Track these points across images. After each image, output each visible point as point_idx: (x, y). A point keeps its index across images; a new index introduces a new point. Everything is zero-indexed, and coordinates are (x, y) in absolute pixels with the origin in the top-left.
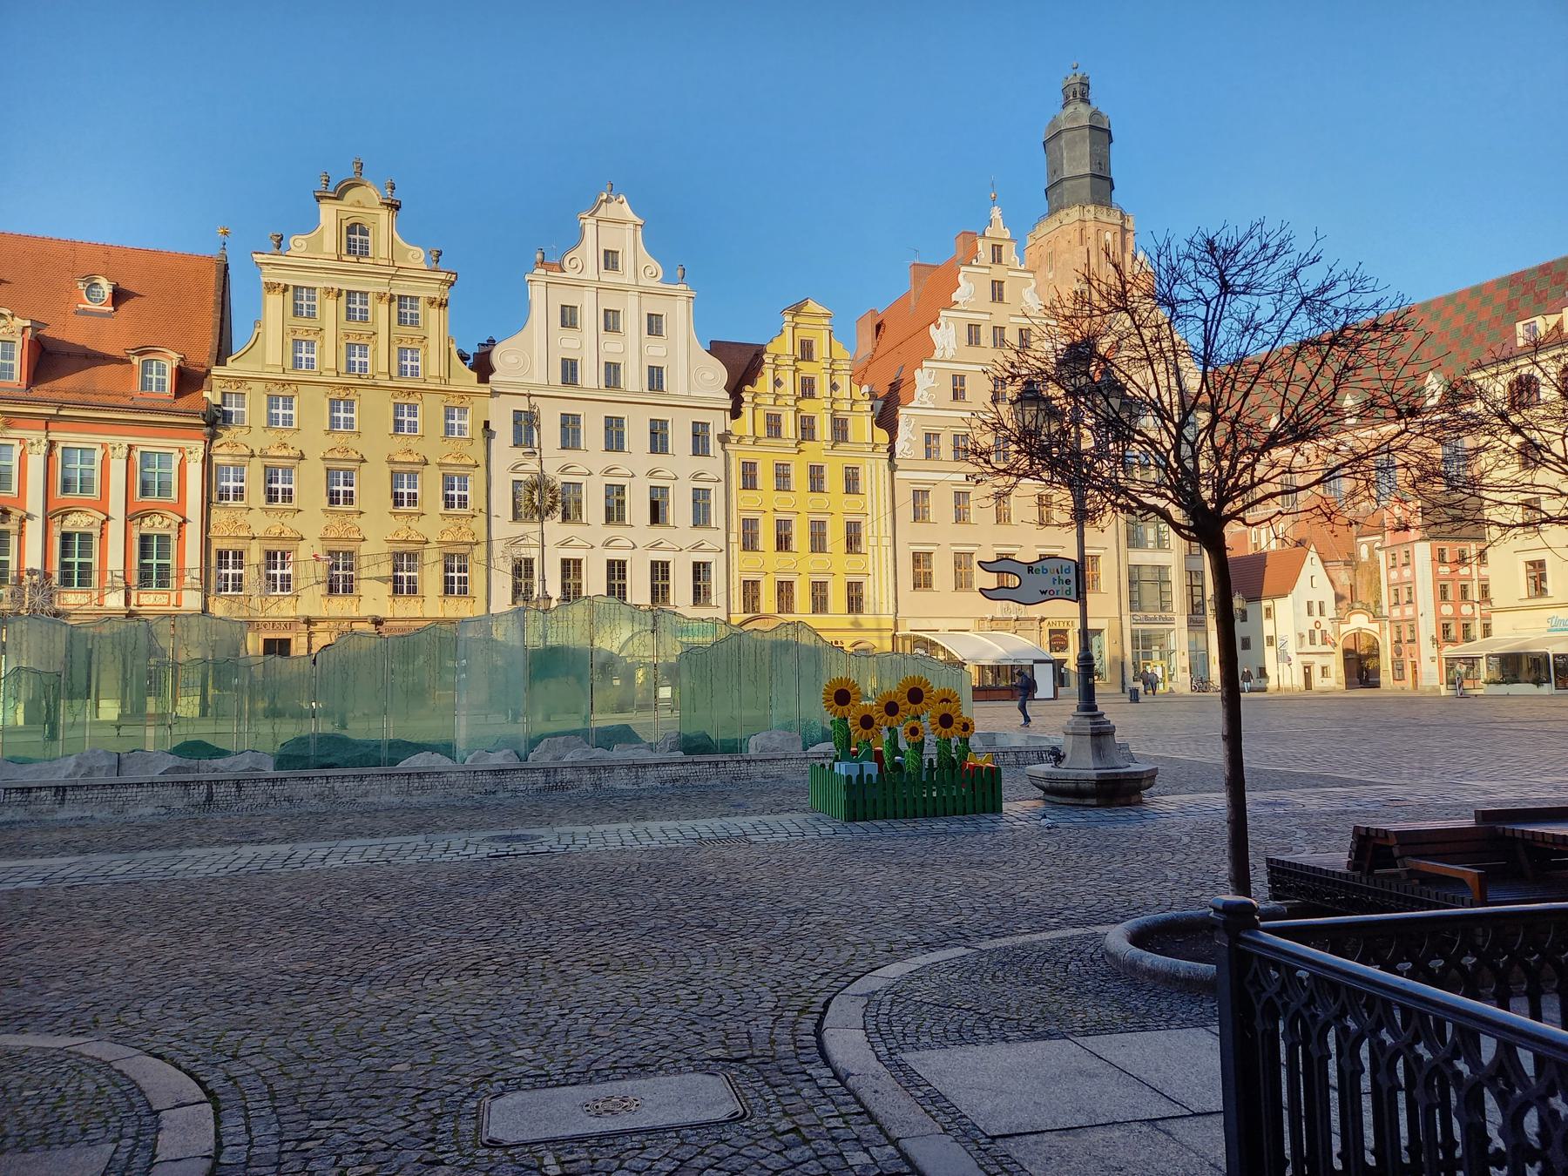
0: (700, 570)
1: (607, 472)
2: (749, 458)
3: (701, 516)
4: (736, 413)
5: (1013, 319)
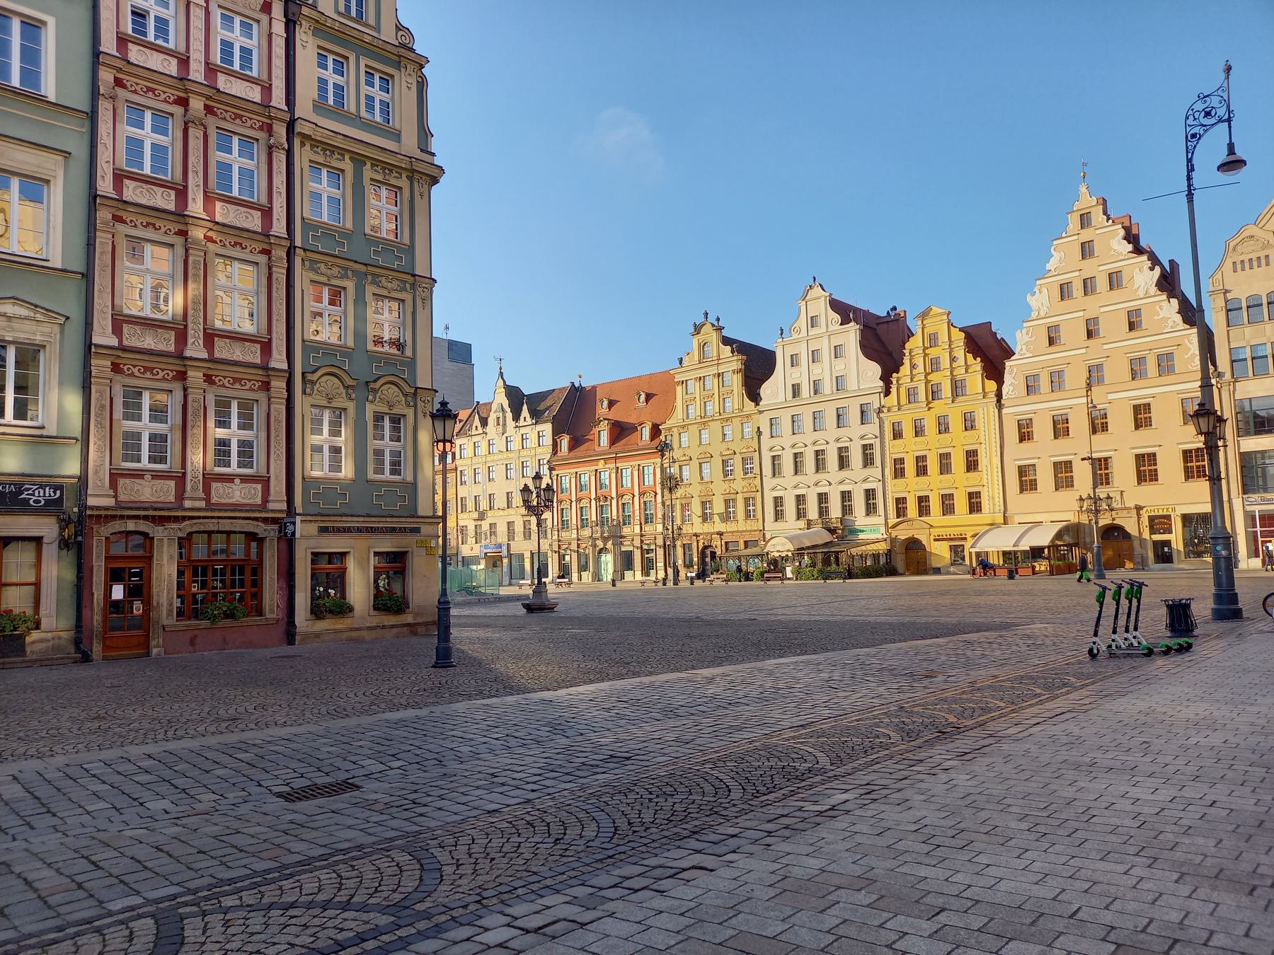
0: (870, 494)
1: (793, 446)
2: (896, 419)
3: (868, 461)
4: (887, 393)
5: (1101, 268)
